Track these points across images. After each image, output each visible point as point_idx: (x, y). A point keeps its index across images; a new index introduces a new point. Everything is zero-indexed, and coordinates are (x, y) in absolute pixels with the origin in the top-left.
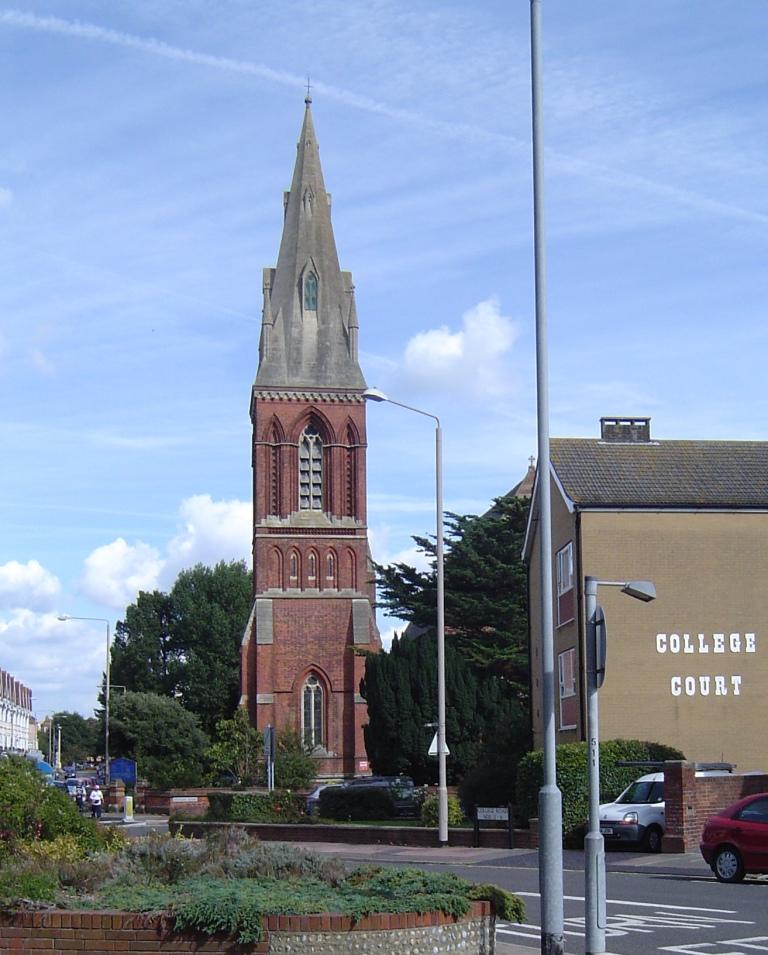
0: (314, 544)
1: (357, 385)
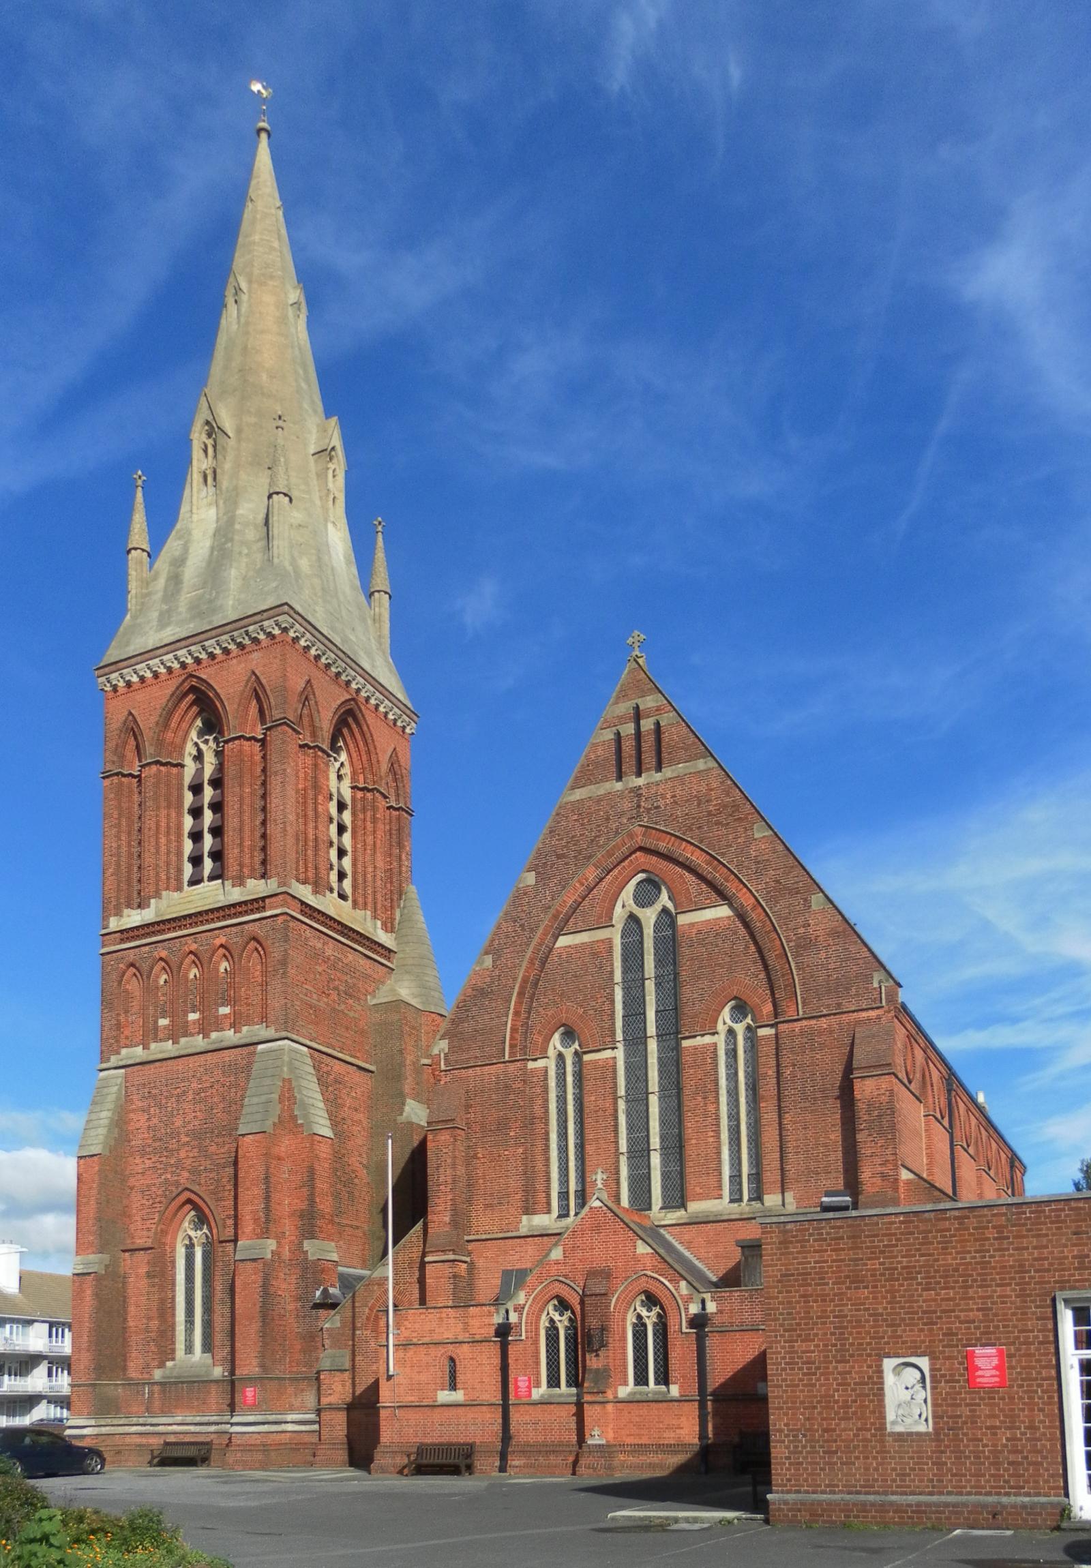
0: (194, 947)
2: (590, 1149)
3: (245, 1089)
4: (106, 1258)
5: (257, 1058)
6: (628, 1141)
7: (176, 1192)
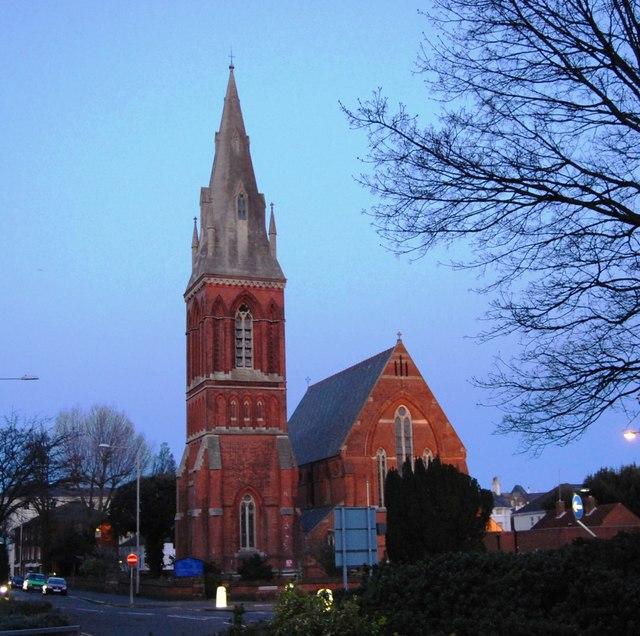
1: (278, 276)
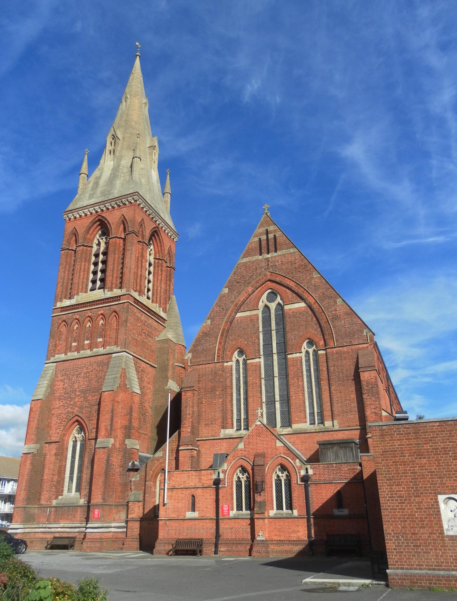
2: (250, 400)
3: (106, 372)
4: (38, 446)
5: (112, 359)
6: (266, 397)
7: (72, 417)
